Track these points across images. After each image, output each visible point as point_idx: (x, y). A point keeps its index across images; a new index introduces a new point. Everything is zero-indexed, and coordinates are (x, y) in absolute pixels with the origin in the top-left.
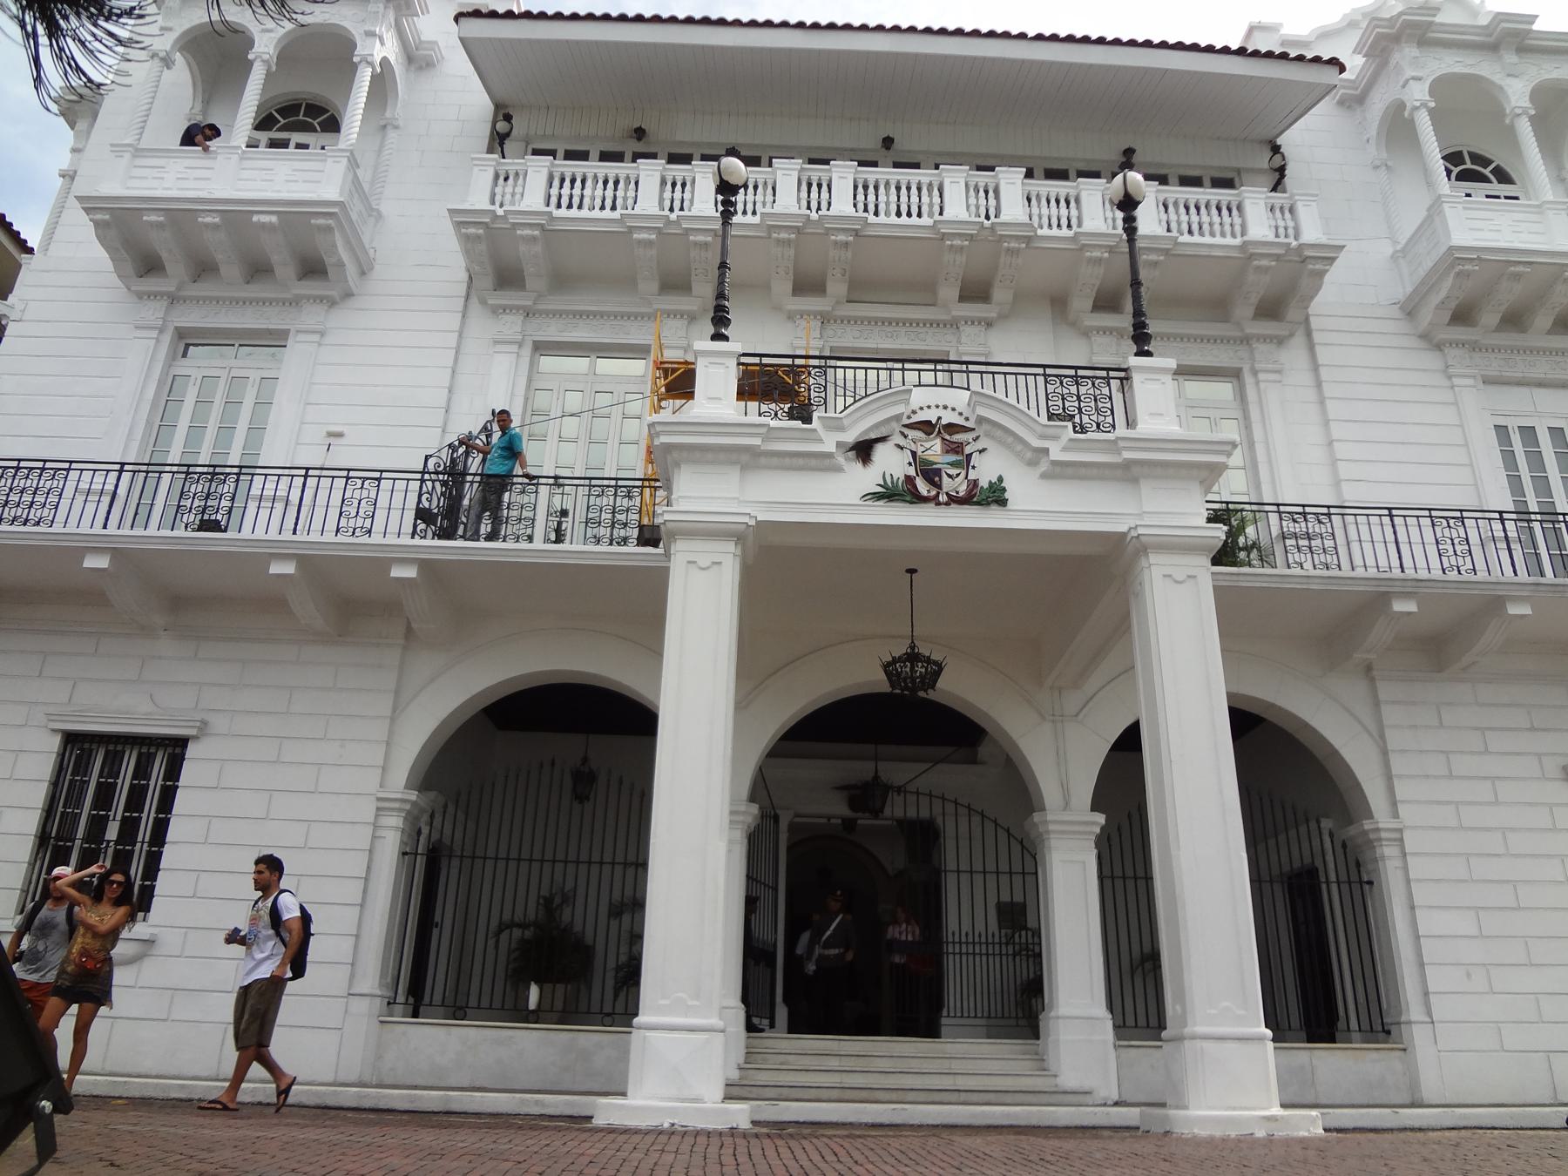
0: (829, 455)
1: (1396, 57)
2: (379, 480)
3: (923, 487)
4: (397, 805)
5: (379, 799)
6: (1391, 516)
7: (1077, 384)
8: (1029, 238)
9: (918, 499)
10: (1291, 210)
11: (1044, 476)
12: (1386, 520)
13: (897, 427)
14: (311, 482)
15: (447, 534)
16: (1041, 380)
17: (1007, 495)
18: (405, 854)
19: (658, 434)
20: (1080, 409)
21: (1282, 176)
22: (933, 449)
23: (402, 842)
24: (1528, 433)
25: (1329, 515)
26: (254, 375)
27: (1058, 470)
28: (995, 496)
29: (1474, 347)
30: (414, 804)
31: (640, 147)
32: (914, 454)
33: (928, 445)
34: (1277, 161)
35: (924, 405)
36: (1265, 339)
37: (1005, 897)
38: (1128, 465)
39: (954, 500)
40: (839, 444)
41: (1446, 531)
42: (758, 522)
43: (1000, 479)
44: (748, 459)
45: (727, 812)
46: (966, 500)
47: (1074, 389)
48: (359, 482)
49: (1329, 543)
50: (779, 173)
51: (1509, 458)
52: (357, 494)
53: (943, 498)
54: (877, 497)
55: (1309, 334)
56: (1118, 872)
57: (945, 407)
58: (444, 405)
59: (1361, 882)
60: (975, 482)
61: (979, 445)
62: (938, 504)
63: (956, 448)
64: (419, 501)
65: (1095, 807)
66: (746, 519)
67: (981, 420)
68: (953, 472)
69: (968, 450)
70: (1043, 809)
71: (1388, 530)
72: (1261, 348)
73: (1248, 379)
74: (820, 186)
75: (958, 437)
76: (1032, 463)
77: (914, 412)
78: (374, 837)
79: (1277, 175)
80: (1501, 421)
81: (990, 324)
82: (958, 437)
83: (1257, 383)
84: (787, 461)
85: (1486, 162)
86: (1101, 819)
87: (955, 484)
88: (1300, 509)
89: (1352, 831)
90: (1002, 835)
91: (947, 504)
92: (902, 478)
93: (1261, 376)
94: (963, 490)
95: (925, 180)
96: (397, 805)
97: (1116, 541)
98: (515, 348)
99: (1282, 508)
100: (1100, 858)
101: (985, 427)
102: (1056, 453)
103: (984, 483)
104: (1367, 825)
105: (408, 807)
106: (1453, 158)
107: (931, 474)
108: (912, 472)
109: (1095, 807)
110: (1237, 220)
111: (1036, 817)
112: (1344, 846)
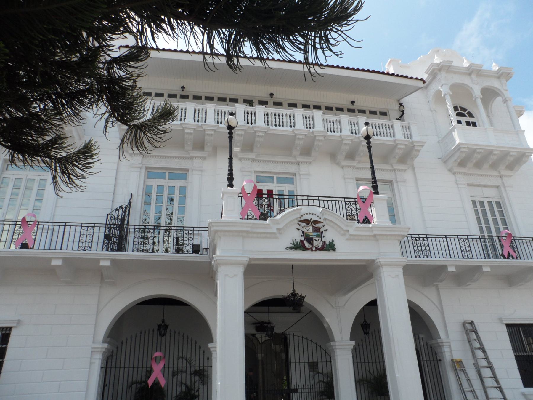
0: (274, 233)
1: (439, 77)
2: (94, 227)
3: (307, 245)
4: (100, 350)
5: (93, 348)
6: (446, 238)
7: (356, 204)
8: (325, 137)
9: (305, 249)
10: (408, 128)
11: (347, 239)
12: (445, 239)
13: (296, 222)
14: (67, 228)
15: (121, 247)
16: (344, 203)
17: (335, 247)
18: (102, 368)
19: (213, 226)
20: (357, 214)
21: (403, 113)
22: (309, 230)
23: (102, 364)
24: (482, 203)
25: (427, 238)
26: (37, 178)
27: (352, 237)
28: (330, 247)
29: (465, 174)
30: (106, 348)
31: (183, 93)
32: (303, 232)
33: (308, 228)
34: (402, 108)
35: (305, 213)
36: (401, 170)
37: (311, 360)
38: (375, 236)
39: (317, 249)
40: (278, 229)
41: (463, 243)
42: (250, 259)
43: (333, 241)
44: (245, 235)
47: (354, 206)
48: (86, 228)
49: (427, 248)
50: (237, 109)
51: (476, 211)
52: (85, 233)
53: (314, 249)
54: (291, 248)
55: (413, 169)
56: (359, 361)
57: (313, 214)
58: (113, 191)
59: (437, 360)
60: (325, 242)
61: (325, 228)
62: (312, 251)
63: (317, 230)
64: (105, 232)
65: (351, 339)
66: (246, 259)
67: (325, 219)
68: (317, 239)
69: (321, 230)
70: (334, 341)
71: (446, 243)
72: (398, 173)
73: (395, 184)
74: (251, 114)
75: (318, 225)
76: (343, 235)
77: (302, 216)
78: (91, 363)
79: (401, 113)
80: (474, 199)
81: (310, 163)
82: (318, 225)
83: (398, 186)
84: (259, 235)
85: (465, 110)
86: (353, 343)
87: (317, 243)
88: (418, 236)
89: (433, 342)
90: (319, 348)
91: (315, 251)
92: (299, 241)
93: (399, 183)
94: (320, 245)
95: (288, 114)
96: (100, 350)
97: (372, 262)
98: (139, 170)
99: (412, 236)
100: (353, 356)
101: (327, 222)
102: (352, 232)
103: (327, 243)
104: (439, 341)
105: (104, 350)
106: (456, 108)
107: (310, 240)
108: (302, 239)
109: (351, 339)
110: (392, 131)
111: (332, 343)
112: (431, 347)
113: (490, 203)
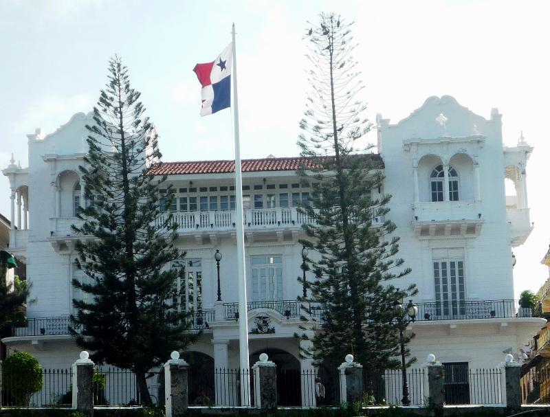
3: (259, 331)
9: (257, 333)
24: (444, 264)
28: (272, 331)
39: (265, 333)
45: (241, 327)
46: (267, 333)
51: (436, 273)
87: (265, 330)
113: (452, 264)
